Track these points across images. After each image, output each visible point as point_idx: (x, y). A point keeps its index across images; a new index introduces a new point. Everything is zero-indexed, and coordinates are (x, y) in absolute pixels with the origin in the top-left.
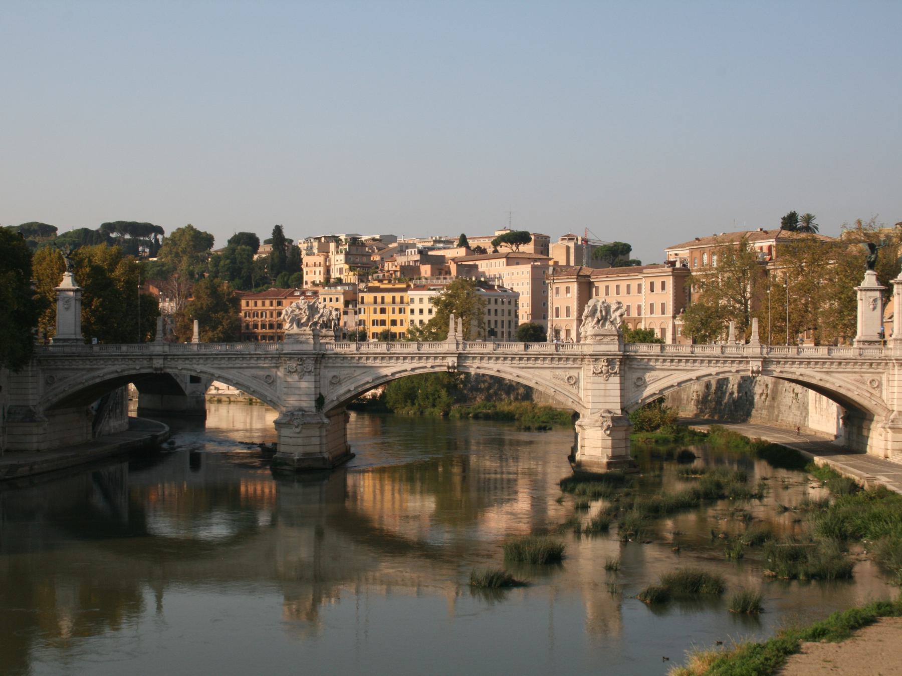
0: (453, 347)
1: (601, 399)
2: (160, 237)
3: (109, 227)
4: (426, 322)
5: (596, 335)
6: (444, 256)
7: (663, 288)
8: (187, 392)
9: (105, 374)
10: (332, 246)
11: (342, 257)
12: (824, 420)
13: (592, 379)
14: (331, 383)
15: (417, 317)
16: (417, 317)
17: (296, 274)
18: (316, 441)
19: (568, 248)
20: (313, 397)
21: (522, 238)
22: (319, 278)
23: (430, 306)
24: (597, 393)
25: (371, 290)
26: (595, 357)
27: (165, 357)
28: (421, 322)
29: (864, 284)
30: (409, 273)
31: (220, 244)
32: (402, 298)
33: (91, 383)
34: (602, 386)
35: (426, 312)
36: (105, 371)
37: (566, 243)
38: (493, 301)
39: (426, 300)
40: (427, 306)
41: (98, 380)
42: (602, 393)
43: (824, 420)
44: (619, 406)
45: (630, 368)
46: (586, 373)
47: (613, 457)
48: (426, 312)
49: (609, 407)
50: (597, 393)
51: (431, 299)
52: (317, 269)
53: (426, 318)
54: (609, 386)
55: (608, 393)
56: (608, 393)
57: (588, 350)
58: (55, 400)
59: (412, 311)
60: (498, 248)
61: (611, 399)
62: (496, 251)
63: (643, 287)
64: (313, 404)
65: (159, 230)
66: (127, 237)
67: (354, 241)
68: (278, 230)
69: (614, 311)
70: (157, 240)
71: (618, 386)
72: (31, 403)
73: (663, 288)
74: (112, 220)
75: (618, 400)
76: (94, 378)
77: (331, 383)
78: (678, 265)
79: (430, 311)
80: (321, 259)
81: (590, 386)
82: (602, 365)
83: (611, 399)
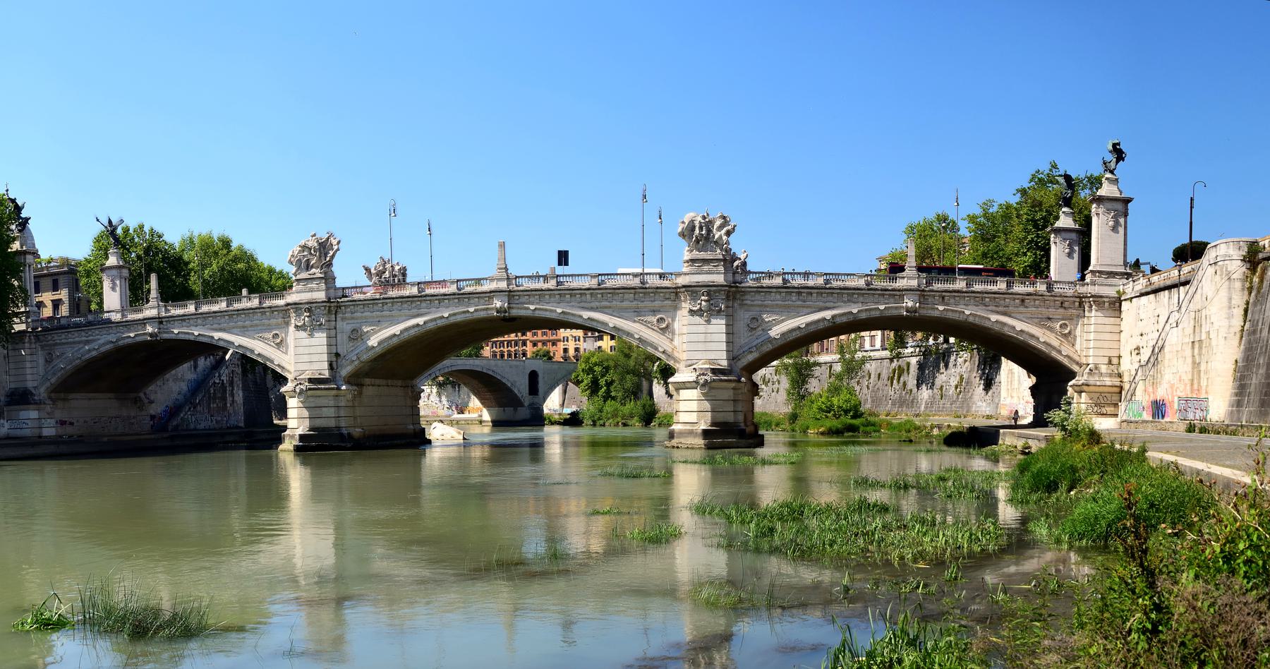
5: (693, 261)
9: (100, 346)
27: (159, 320)
34: (702, 329)
36: (101, 341)
41: (94, 353)
44: (724, 355)
45: (742, 305)
49: (712, 356)
54: (711, 328)
55: (709, 337)
56: (709, 337)
57: (681, 281)
58: (53, 380)
71: (723, 328)
72: (30, 385)
75: (724, 346)
81: (685, 330)
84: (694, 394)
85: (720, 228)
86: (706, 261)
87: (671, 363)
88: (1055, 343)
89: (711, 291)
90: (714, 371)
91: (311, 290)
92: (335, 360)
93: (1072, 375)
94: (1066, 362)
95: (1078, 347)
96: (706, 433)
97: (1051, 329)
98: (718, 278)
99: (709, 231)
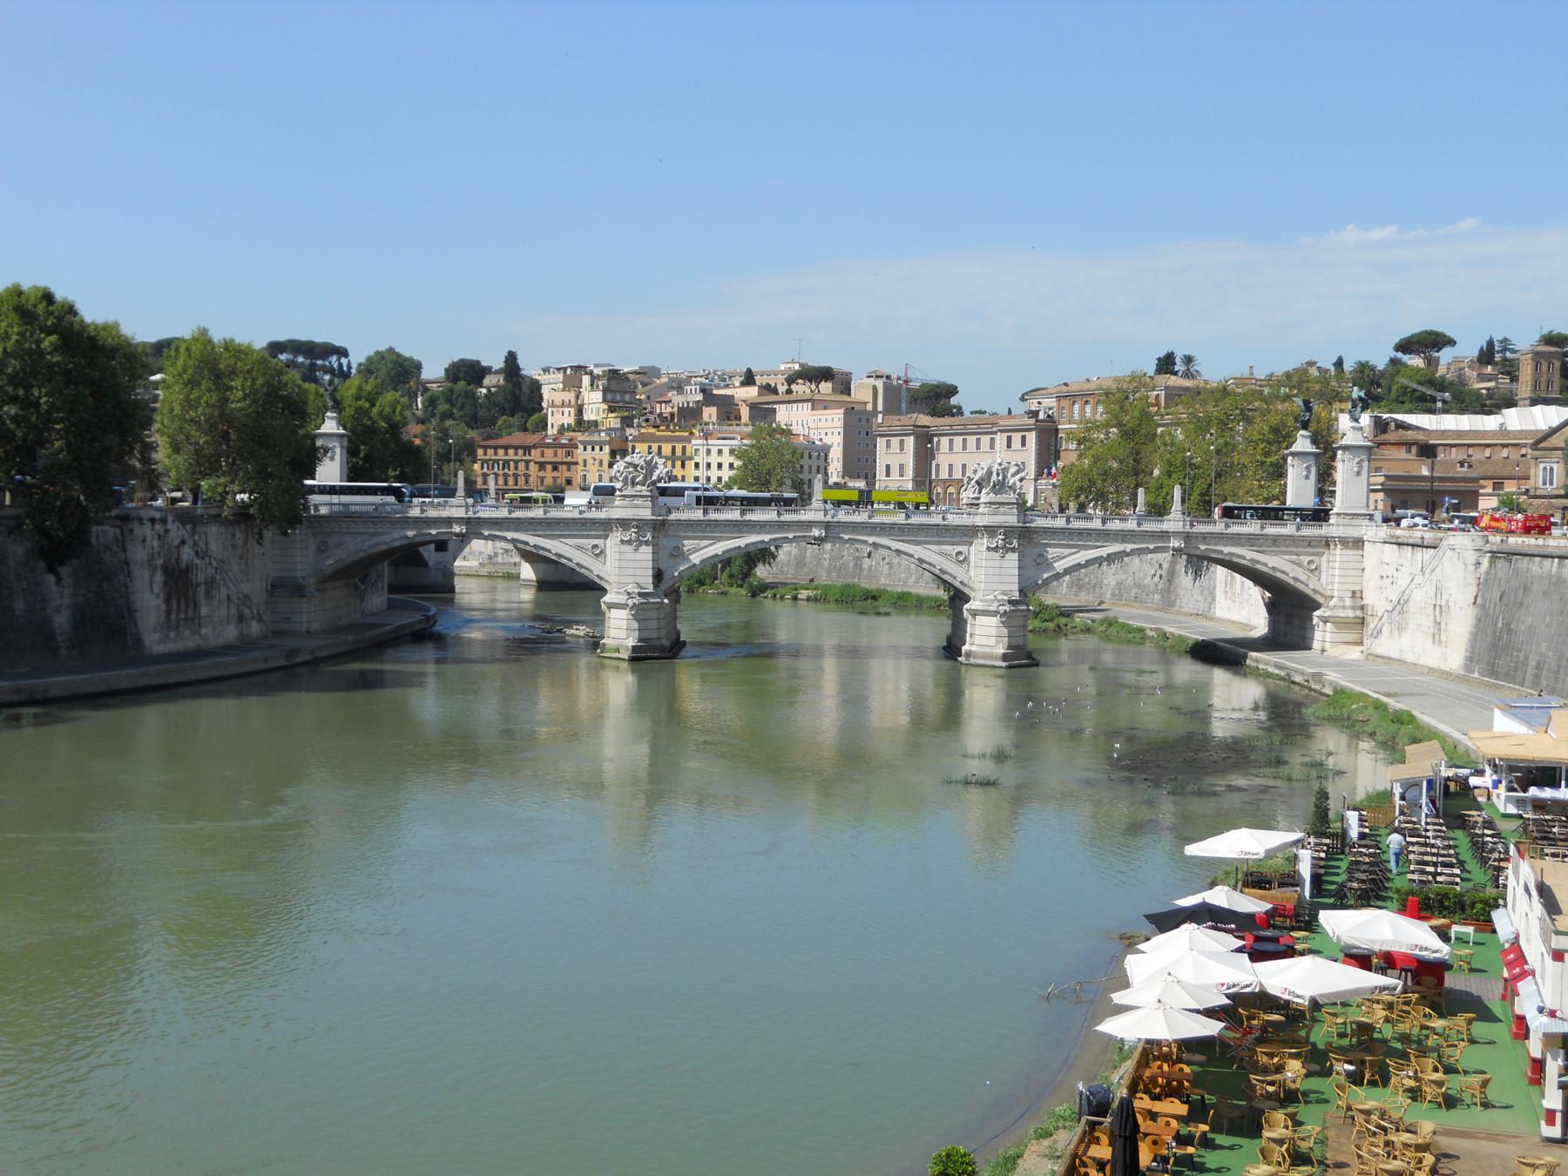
0: (820, 516)
1: (996, 579)
2: (344, 361)
3: (276, 348)
4: (725, 479)
6: (732, 397)
7: (1023, 444)
8: (430, 564)
10: (586, 379)
11: (598, 396)
12: (1241, 610)
13: (985, 554)
14: (672, 555)
15: (714, 474)
16: (714, 474)
17: (535, 417)
18: (654, 624)
19: (875, 389)
20: (650, 572)
21: (825, 374)
22: (568, 418)
23: (732, 459)
24: (991, 571)
25: (641, 438)
26: (990, 530)
28: (720, 479)
29: (1295, 448)
30: (689, 415)
31: (433, 371)
32: (684, 448)
33: (376, 550)
34: (997, 564)
35: (726, 466)
37: (872, 380)
38: (806, 455)
39: (726, 451)
40: (727, 459)
41: (384, 547)
42: (997, 571)
43: (1241, 610)
44: (1016, 587)
46: (979, 549)
47: (1009, 647)
48: (726, 466)
50: (991, 571)
51: (732, 452)
52: (566, 410)
53: (726, 474)
54: (1006, 563)
57: (980, 521)
59: (697, 465)
60: (793, 387)
61: (1008, 579)
62: (789, 392)
63: (998, 442)
64: (650, 580)
65: (343, 353)
66: (300, 359)
67: (614, 375)
68: (511, 358)
69: (1014, 475)
70: (340, 365)
71: (1016, 564)
72: (299, 574)
73: (1023, 444)
74: (282, 337)
75: (1016, 579)
76: (379, 544)
77: (672, 555)
78: (1041, 416)
79: (731, 466)
80: (570, 396)
82: (999, 540)
83: (1008, 579)
84: (994, 621)
85: (1014, 475)
86: (1001, 504)
87: (966, 590)
88: (1303, 577)
89: (1009, 531)
90: (1011, 602)
91: (637, 507)
92: (658, 576)
93: (1317, 606)
94: (1311, 594)
95: (1323, 580)
96: (1005, 657)
97: (1299, 565)
98: (1012, 519)
99: (1005, 477)
